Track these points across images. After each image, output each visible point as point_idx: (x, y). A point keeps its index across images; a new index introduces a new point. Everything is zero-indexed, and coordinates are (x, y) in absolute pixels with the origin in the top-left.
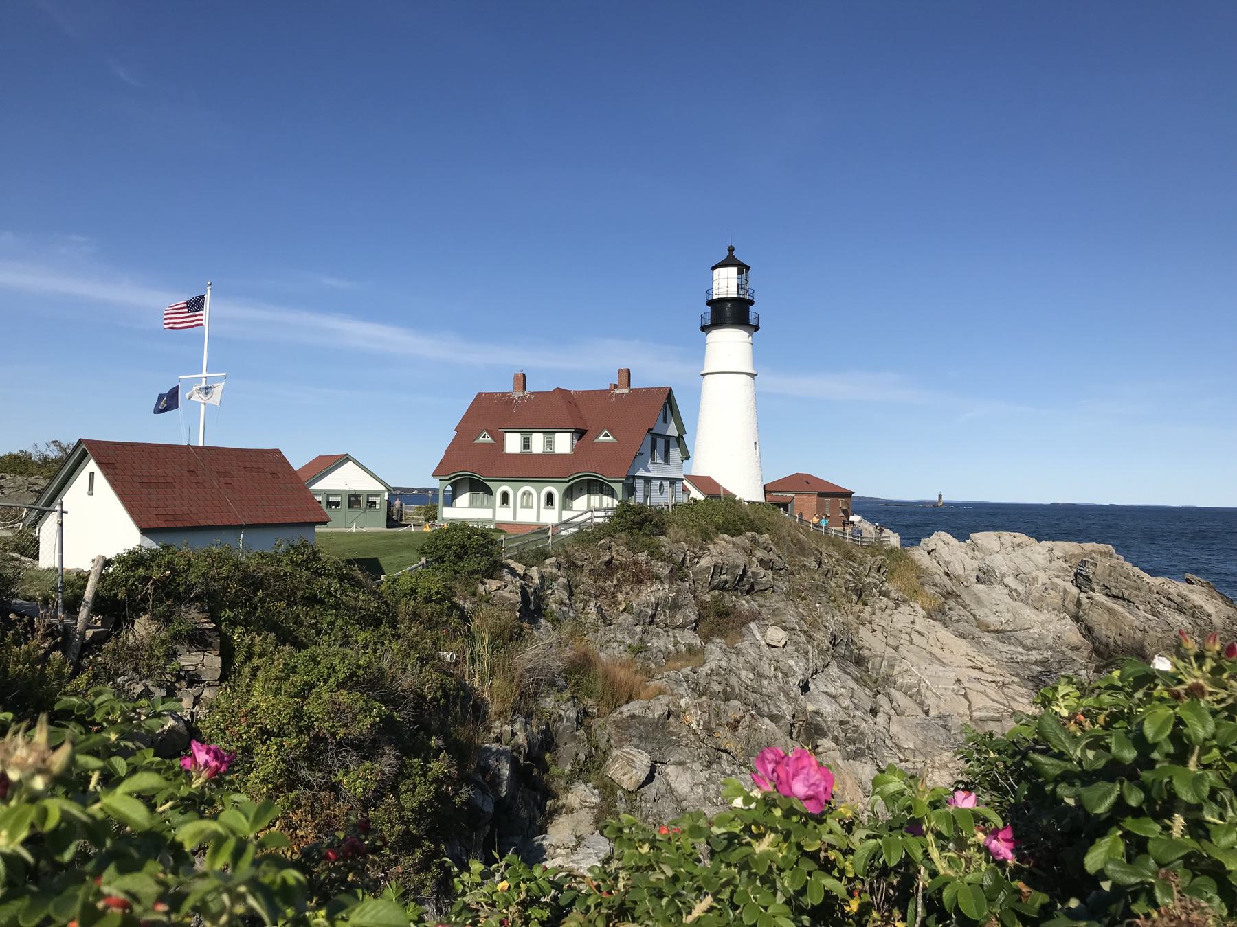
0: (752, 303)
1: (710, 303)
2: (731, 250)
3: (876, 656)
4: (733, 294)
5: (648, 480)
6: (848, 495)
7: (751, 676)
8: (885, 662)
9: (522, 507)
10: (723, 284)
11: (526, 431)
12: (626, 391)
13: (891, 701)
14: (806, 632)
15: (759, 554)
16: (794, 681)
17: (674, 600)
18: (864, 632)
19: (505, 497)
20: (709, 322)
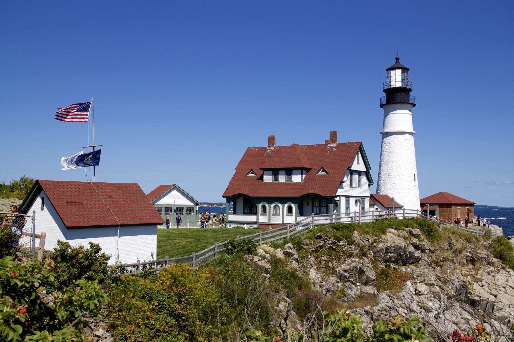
0: (411, 90)
1: (385, 91)
2: (397, 59)
3: (483, 300)
5: (348, 197)
6: (472, 205)
7: (406, 311)
8: (489, 304)
9: (273, 215)
10: (392, 79)
13: (492, 326)
14: (440, 286)
15: (414, 240)
16: (432, 315)
17: (360, 269)
18: (476, 286)
19: (264, 208)
20: (385, 102)
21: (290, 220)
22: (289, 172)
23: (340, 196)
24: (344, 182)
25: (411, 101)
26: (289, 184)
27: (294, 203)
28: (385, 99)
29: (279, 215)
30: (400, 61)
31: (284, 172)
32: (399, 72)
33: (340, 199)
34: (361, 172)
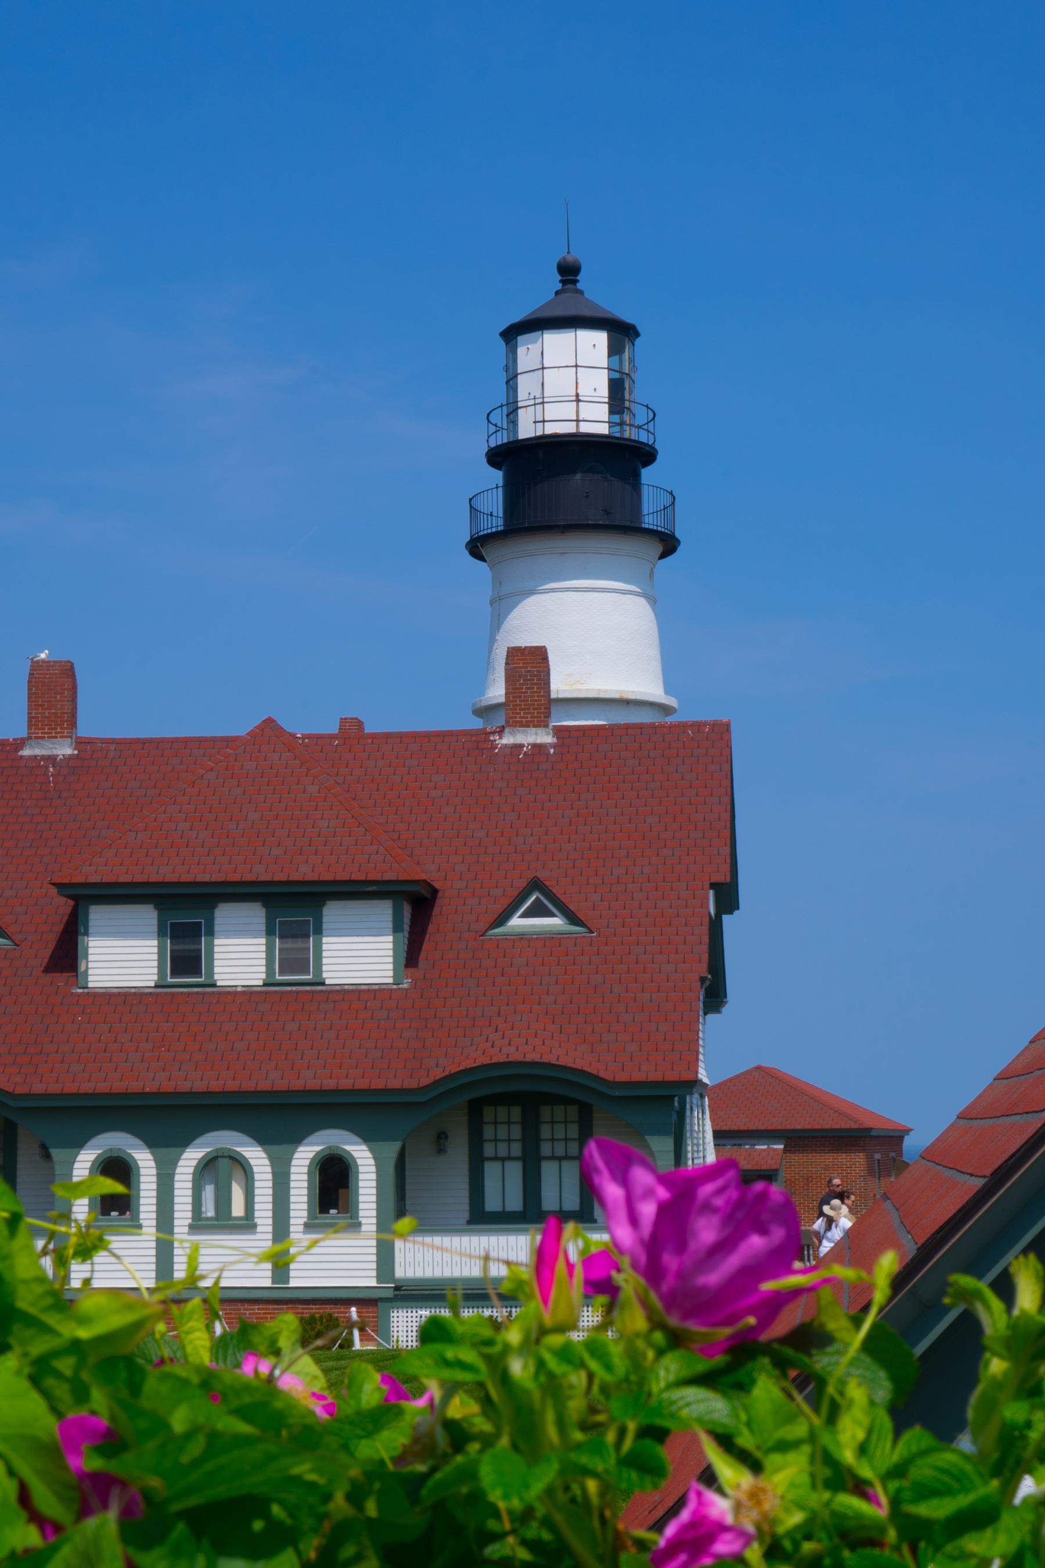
4: (596, 420)
9: (199, 1224)
10: (558, 383)
20: (495, 520)
21: (337, 1261)
22: (295, 908)
25: (649, 521)
26: (296, 999)
27: (368, 1137)
28: (494, 504)
29: (247, 1224)
30: (584, 281)
31: (255, 914)
32: (594, 344)
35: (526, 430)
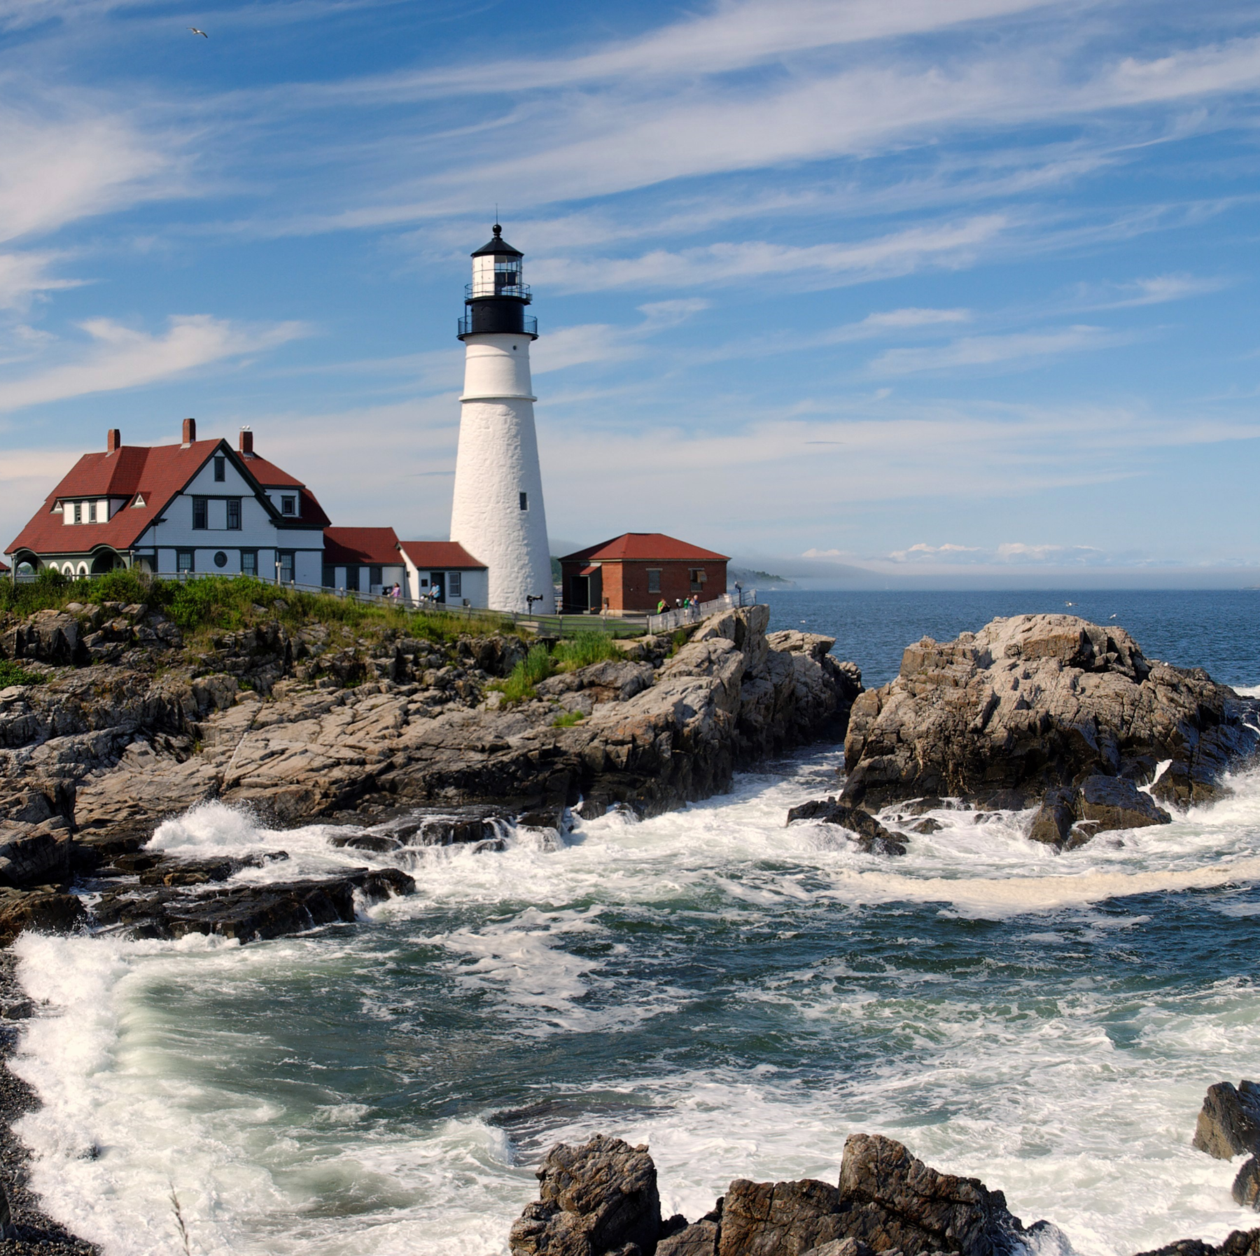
0: (527, 302)
2: (497, 230)
10: (477, 278)
11: (77, 501)
12: (187, 445)
23: (155, 548)
24: (164, 520)
26: (93, 526)
32: (489, 260)
33: (156, 553)
34: (240, 497)
35: (476, 296)
